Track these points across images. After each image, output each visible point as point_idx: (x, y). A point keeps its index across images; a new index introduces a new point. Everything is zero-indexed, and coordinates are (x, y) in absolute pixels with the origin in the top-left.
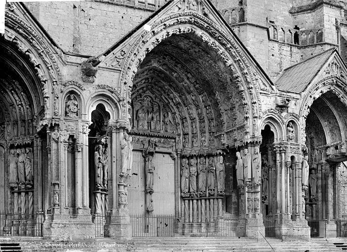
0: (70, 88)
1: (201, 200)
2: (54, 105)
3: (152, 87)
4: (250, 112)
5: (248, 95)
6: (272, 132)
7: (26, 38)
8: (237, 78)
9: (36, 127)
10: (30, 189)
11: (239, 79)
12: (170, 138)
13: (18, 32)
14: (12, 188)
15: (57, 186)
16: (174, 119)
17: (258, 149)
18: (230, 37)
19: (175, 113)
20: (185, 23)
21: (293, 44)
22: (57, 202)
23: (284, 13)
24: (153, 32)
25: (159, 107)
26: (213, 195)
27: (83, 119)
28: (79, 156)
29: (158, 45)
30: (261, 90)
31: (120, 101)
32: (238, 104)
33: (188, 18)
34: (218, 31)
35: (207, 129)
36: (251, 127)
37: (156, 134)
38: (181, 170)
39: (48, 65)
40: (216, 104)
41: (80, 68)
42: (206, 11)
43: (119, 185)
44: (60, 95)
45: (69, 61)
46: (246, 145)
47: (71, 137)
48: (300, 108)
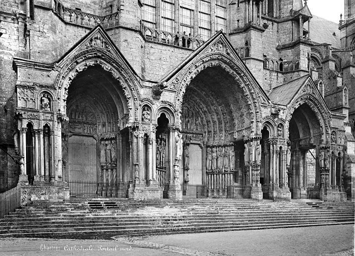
0: (145, 103)
2: (134, 115)
3: (189, 100)
4: (255, 118)
5: (253, 107)
7: (117, 69)
8: (247, 95)
9: (119, 127)
11: (248, 97)
12: (199, 134)
13: (112, 65)
14: (102, 166)
16: (202, 121)
17: (259, 142)
20: (215, 59)
21: (279, 71)
22: (138, 176)
24: (196, 66)
25: (193, 114)
26: (227, 172)
28: (150, 146)
32: (246, 113)
33: (217, 56)
34: (236, 65)
37: (191, 132)
40: (231, 112)
41: (151, 90)
42: (229, 51)
44: (139, 107)
46: (252, 140)
48: (285, 115)
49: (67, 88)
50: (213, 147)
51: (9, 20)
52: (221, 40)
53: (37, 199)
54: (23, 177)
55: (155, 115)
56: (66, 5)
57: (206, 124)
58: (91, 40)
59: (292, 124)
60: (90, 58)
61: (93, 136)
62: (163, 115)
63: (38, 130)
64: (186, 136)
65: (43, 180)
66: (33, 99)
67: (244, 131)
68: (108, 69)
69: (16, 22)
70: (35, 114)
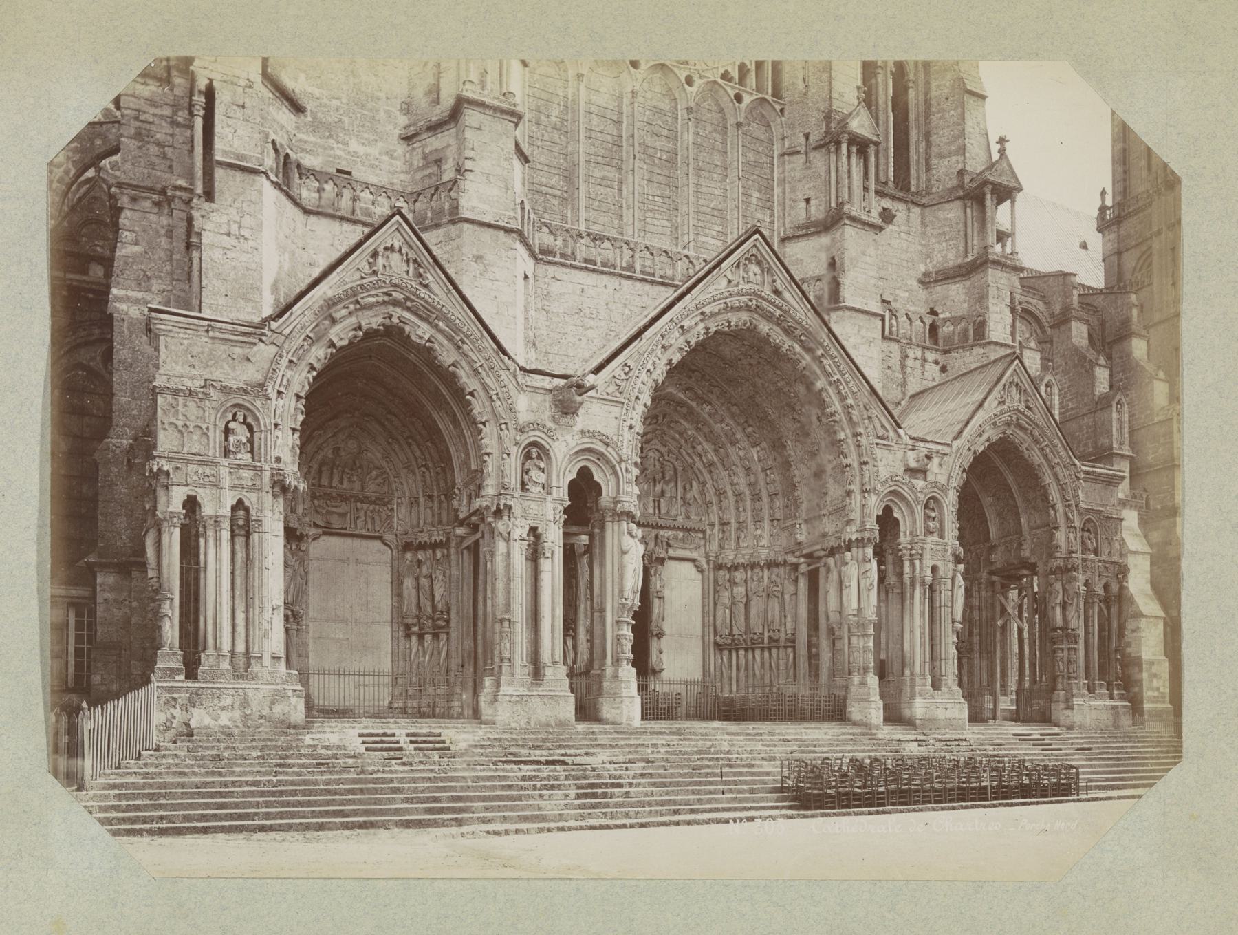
0: (533, 436)
1: (753, 650)
3: (664, 433)
5: (852, 448)
6: (897, 521)
7: (450, 339)
8: (832, 414)
9: (457, 510)
10: (442, 627)
11: (837, 418)
12: (694, 530)
13: (436, 327)
14: (408, 627)
15: (506, 624)
16: (702, 493)
17: (869, 551)
18: (823, 335)
19: (704, 484)
20: (739, 309)
21: (928, 344)
23: (909, 282)
24: (682, 327)
25: (675, 469)
26: (777, 641)
27: (554, 494)
28: (545, 565)
29: (689, 353)
30: (879, 437)
31: (621, 461)
32: (830, 466)
33: (745, 299)
34: (800, 324)
35: (766, 514)
36: (858, 510)
38: (716, 592)
39: (492, 393)
40: (787, 465)
41: (549, 397)
43: (618, 622)
44: (514, 450)
45: (529, 384)
47: (533, 530)
48: (947, 474)
49: (302, 394)
50: (736, 567)
51: (147, 204)
52: (755, 251)
53: (208, 721)
54: (170, 655)
55: (563, 473)
56: (308, 161)
57: (714, 499)
58: (375, 255)
59: (967, 497)
60: (370, 307)
61: (380, 538)
62: (584, 473)
63: (217, 517)
64: (656, 537)
65: (225, 665)
66: (204, 426)
67: (825, 520)
68: (421, 338)
69: (166, 211)
70: (208, 471)
